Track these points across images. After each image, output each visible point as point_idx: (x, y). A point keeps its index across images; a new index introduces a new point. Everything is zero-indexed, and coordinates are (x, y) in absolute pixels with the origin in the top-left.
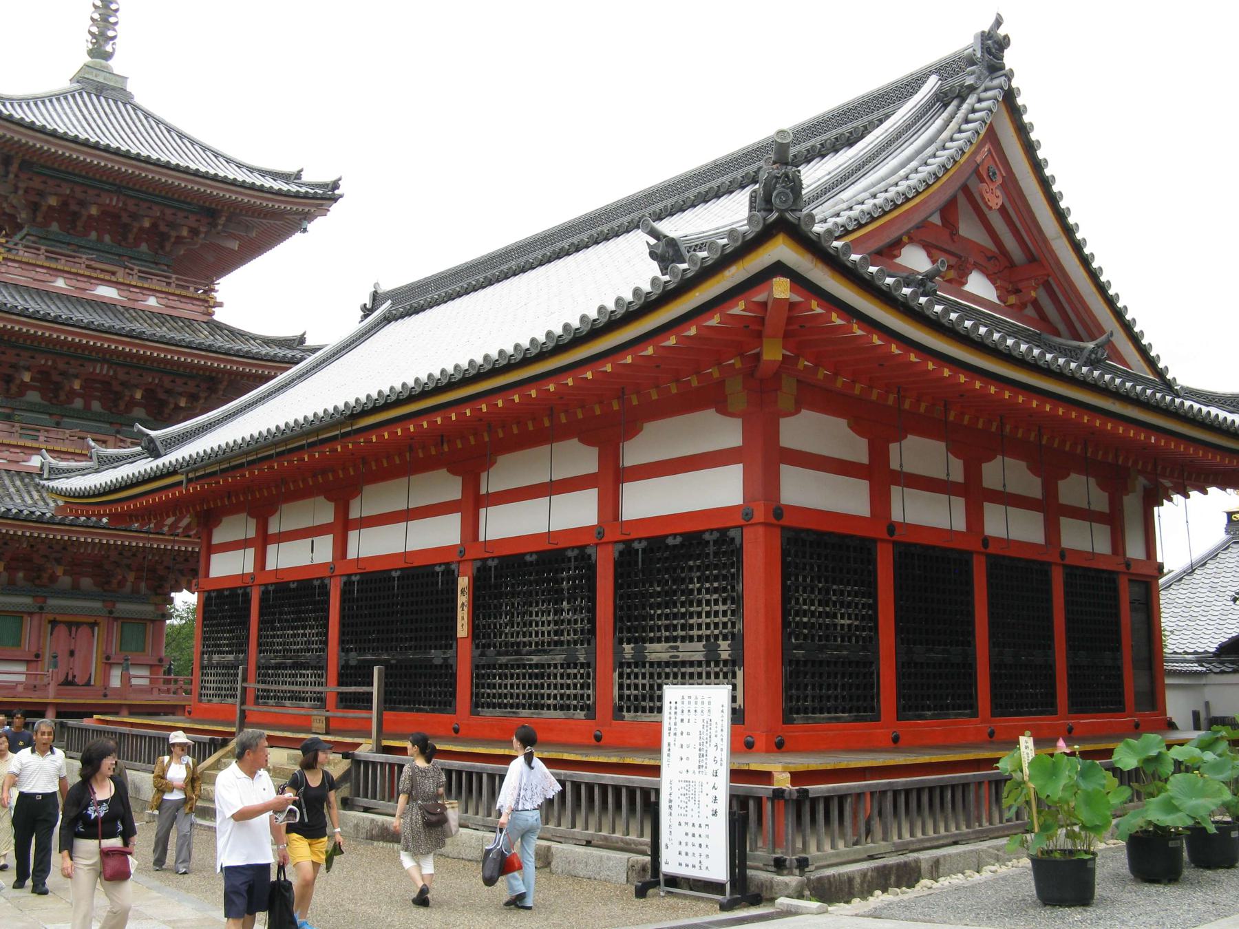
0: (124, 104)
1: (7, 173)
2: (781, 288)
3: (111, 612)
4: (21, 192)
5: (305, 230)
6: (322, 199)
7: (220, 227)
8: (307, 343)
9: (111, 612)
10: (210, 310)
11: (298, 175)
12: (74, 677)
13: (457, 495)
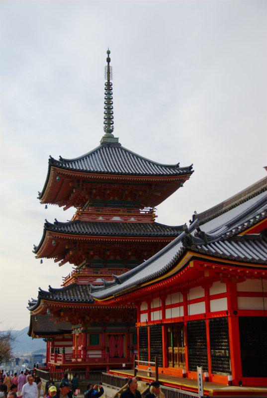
0: (118, 148)
1: (79, 185)
2: (192, 264)
3: (128, 330)
4: (84, 190)
5: (182, 186)
6: (187, 174)
11: (178, 166)
13: (182, 300)
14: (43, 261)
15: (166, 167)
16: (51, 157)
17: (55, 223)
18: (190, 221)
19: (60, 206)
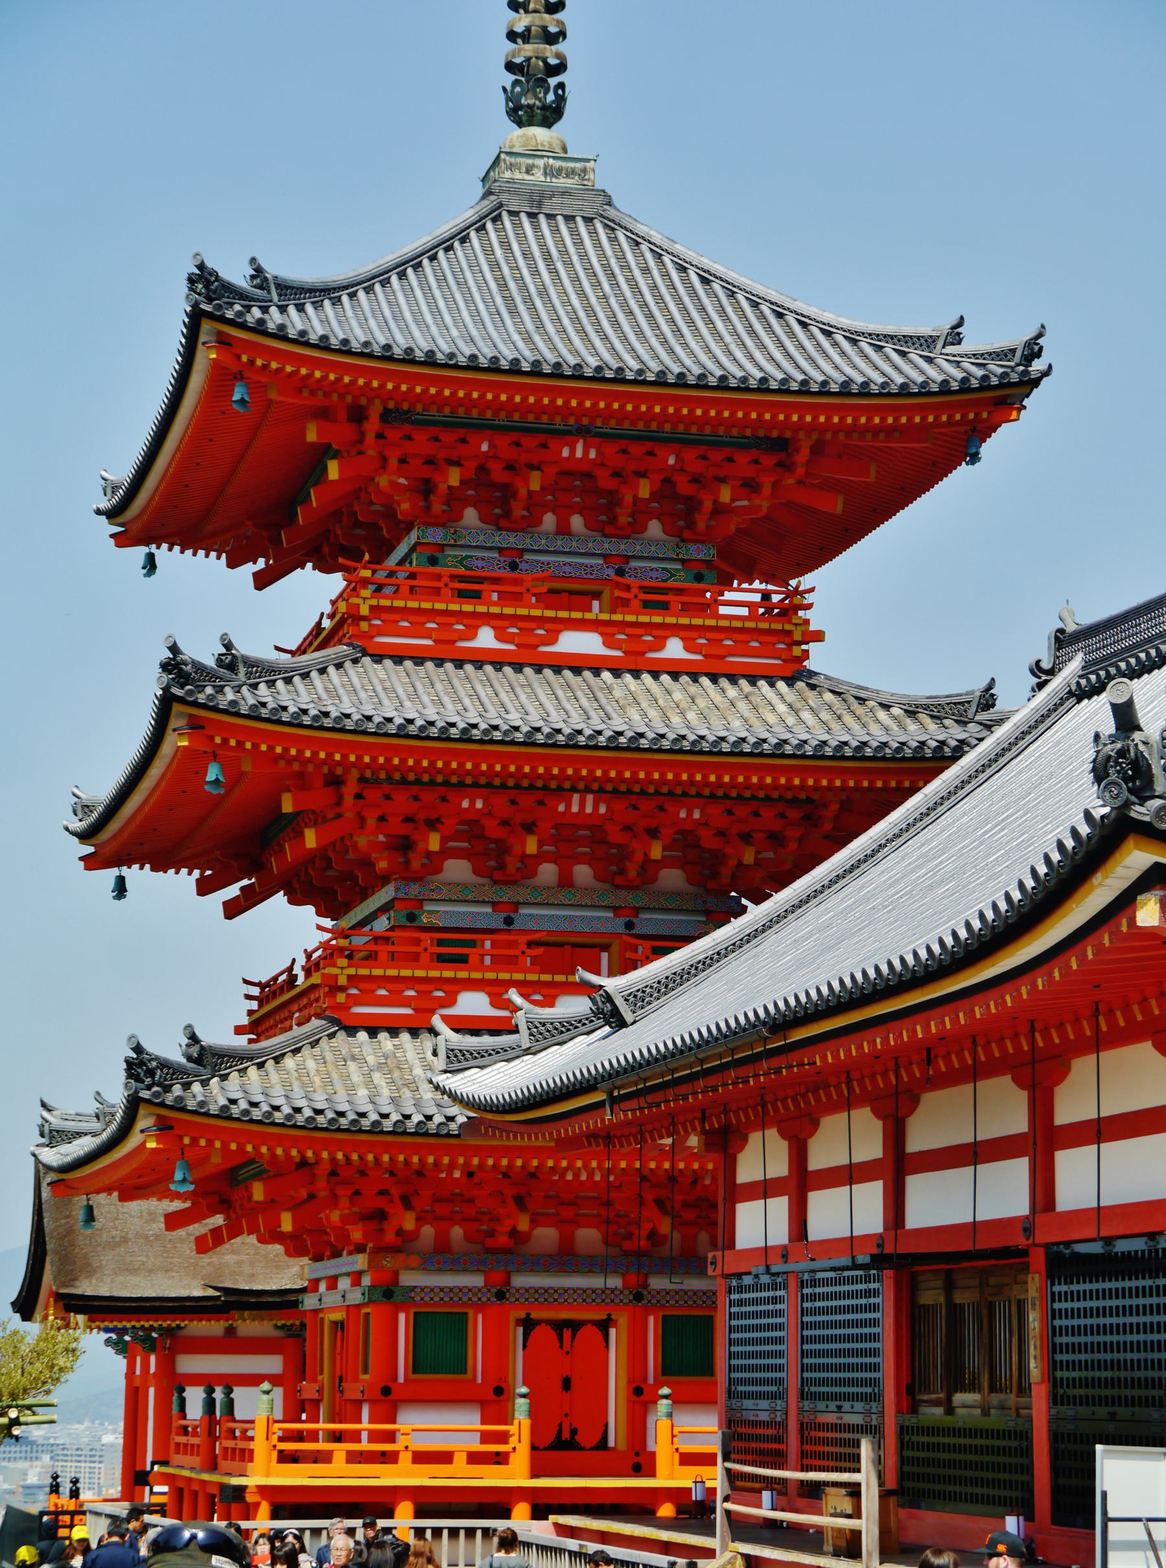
0: (588, 220)
1: (361, 440)
2: (1148, 914)
7: (801, 470)
8: (1000, 705)
9: (638, 1297)
10: (796, 651)
11: (955, 336)
12: (574, 1432)
14: (129, 884)
15: (879, 341)
16: (201, 267)
17: (220, 661)
18: (1037, 669)
19: (232, 564)
